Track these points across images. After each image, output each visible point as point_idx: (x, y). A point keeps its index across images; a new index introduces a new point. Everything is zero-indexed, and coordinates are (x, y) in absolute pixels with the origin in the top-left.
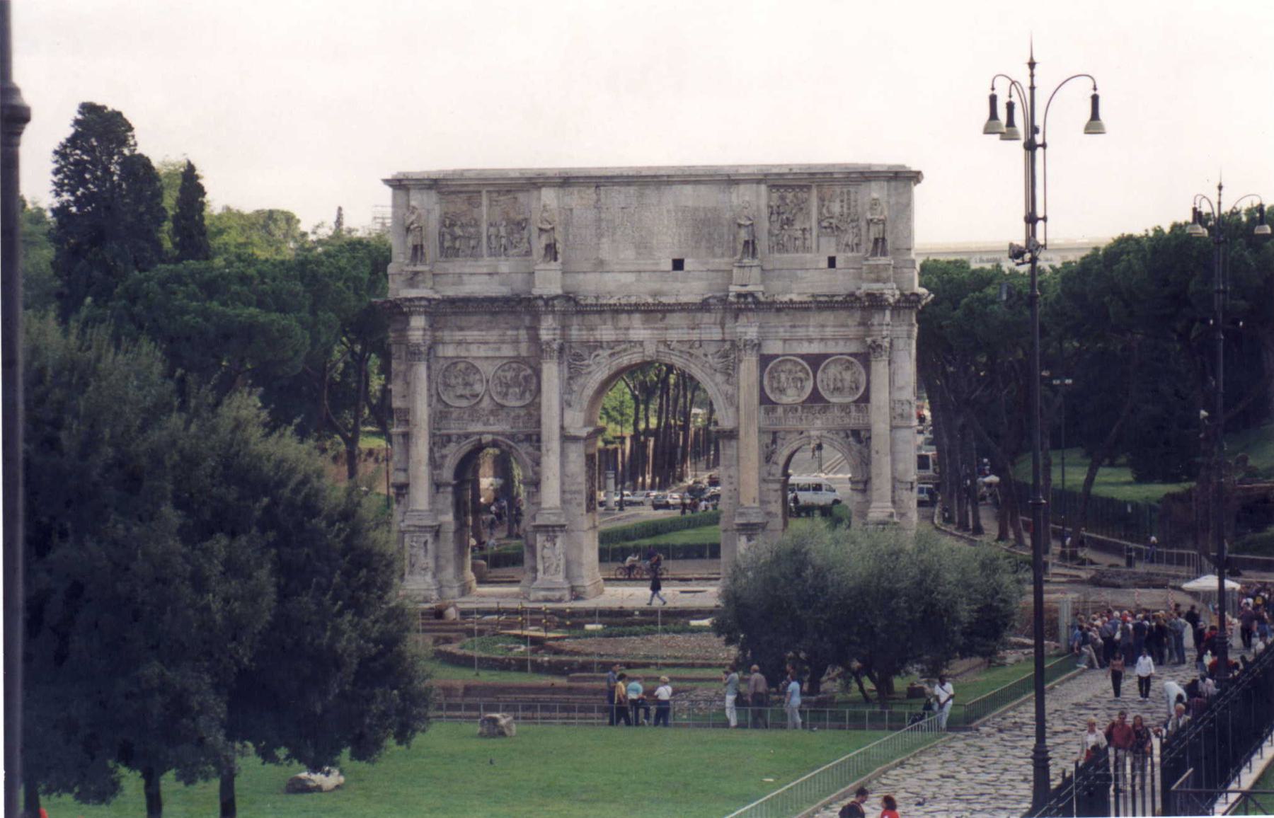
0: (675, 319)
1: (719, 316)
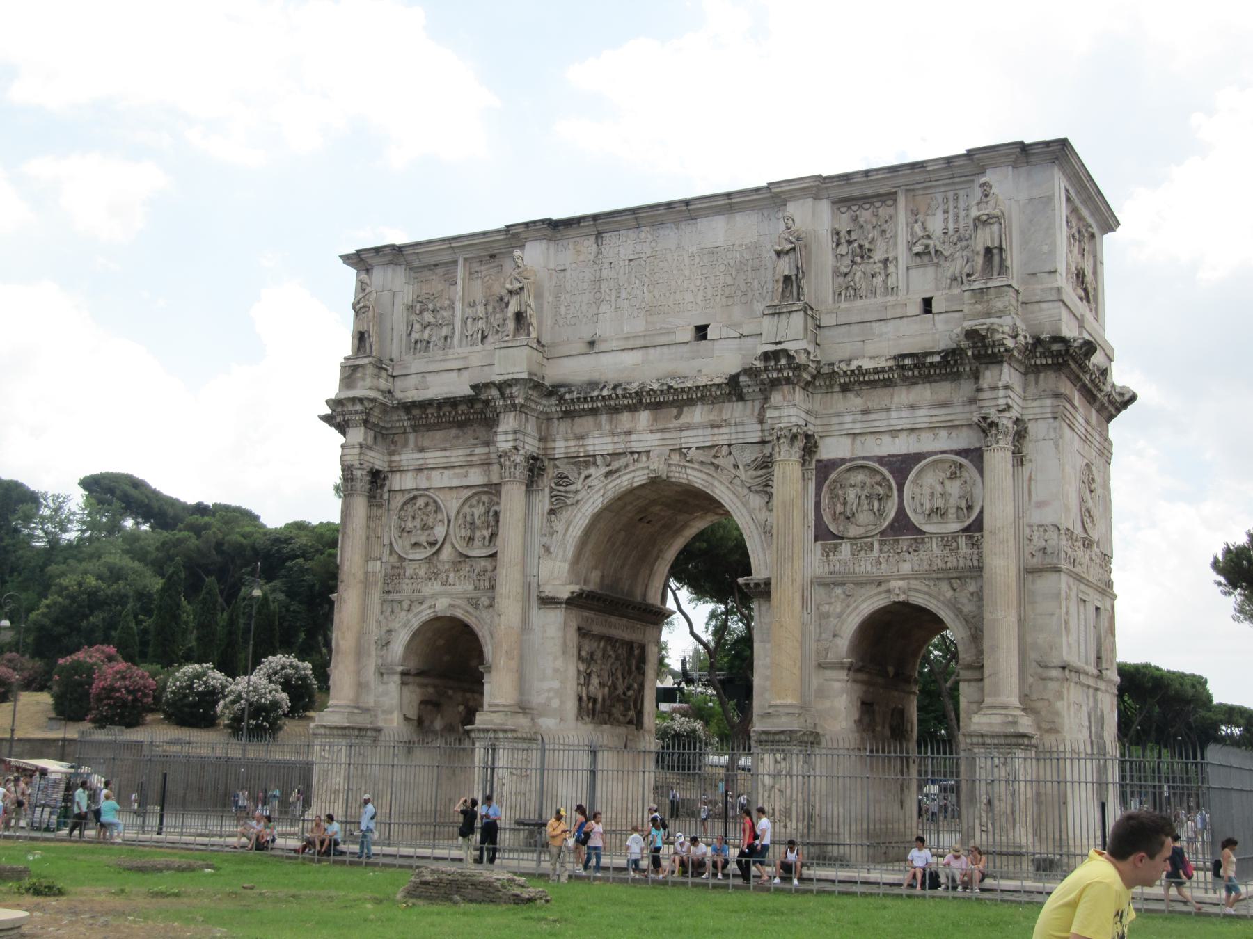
0: (697, 414)
1: (757, 404)
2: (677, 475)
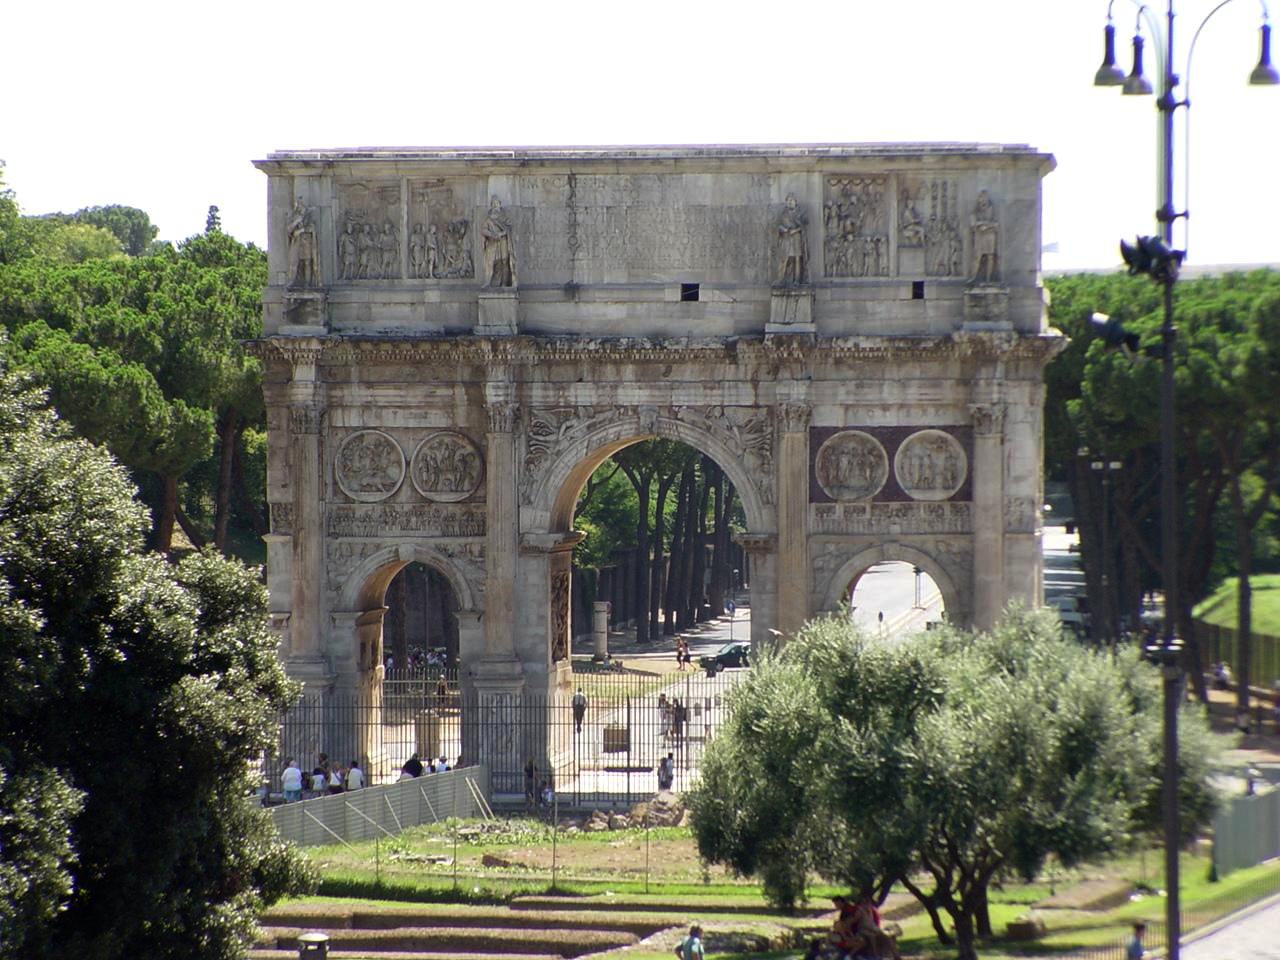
0: (688, 372)
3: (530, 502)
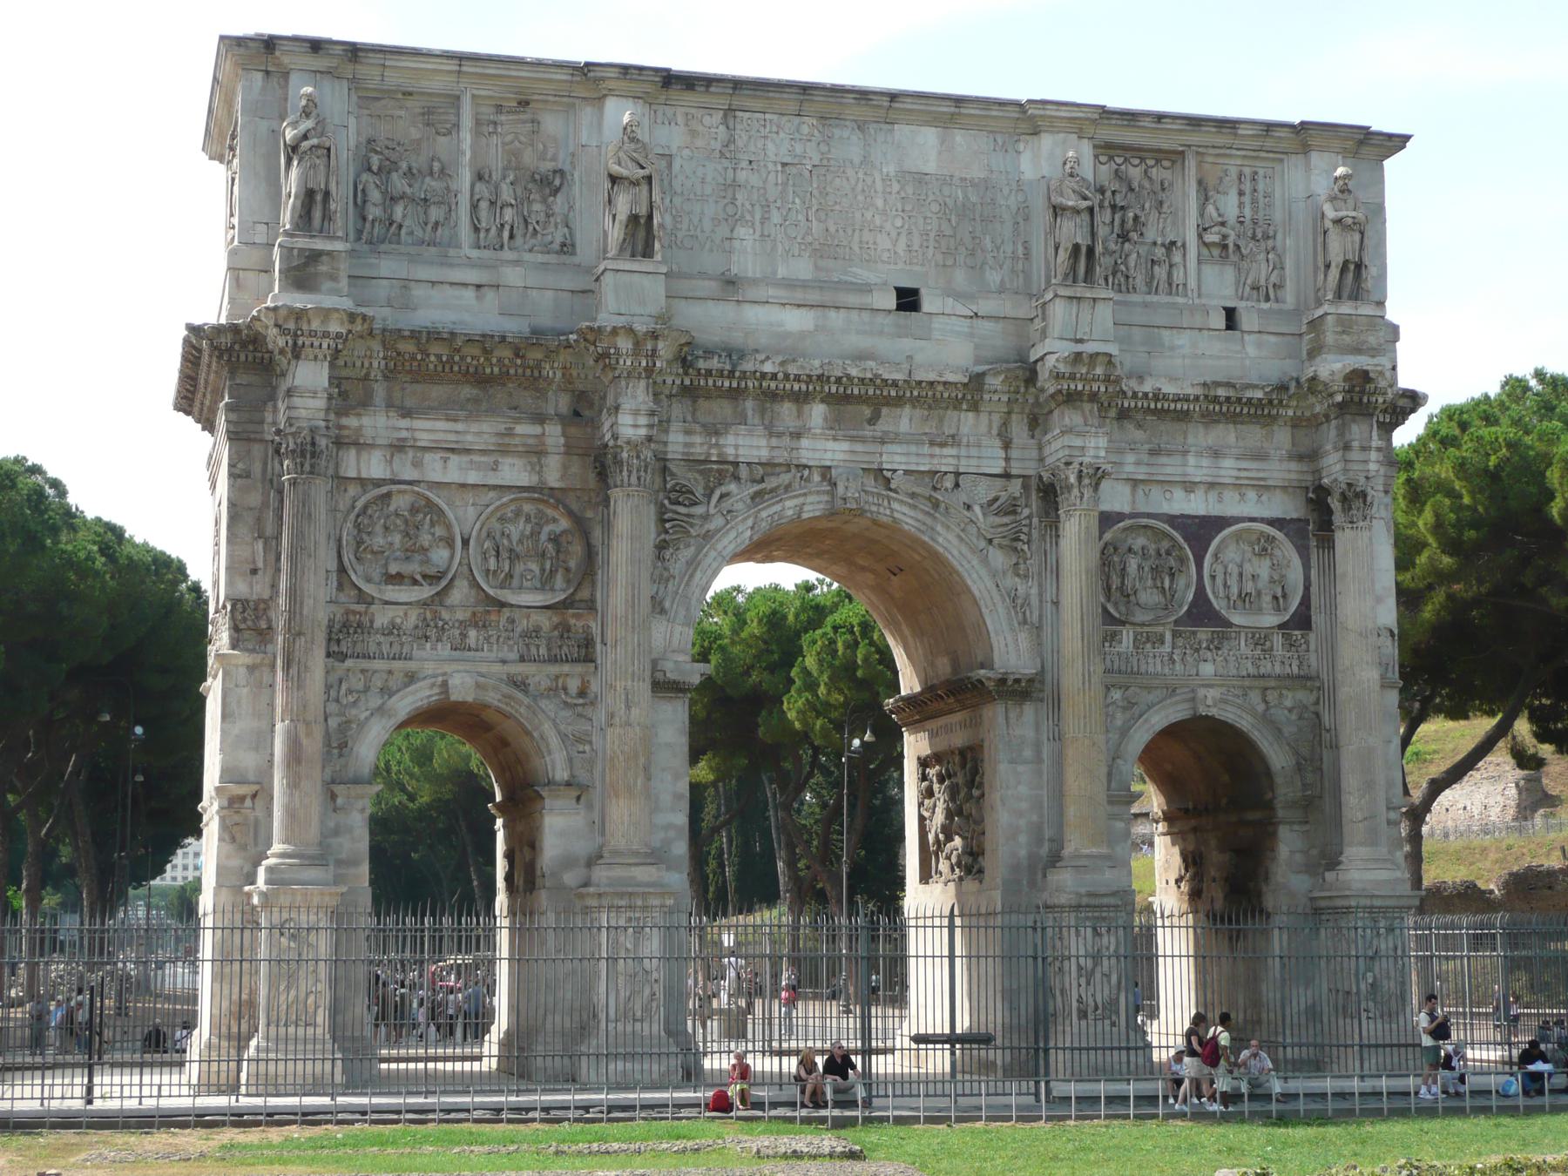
0: (904, 420)
1: (997, 420)
2: (874, 508)
3: (663, 611)
